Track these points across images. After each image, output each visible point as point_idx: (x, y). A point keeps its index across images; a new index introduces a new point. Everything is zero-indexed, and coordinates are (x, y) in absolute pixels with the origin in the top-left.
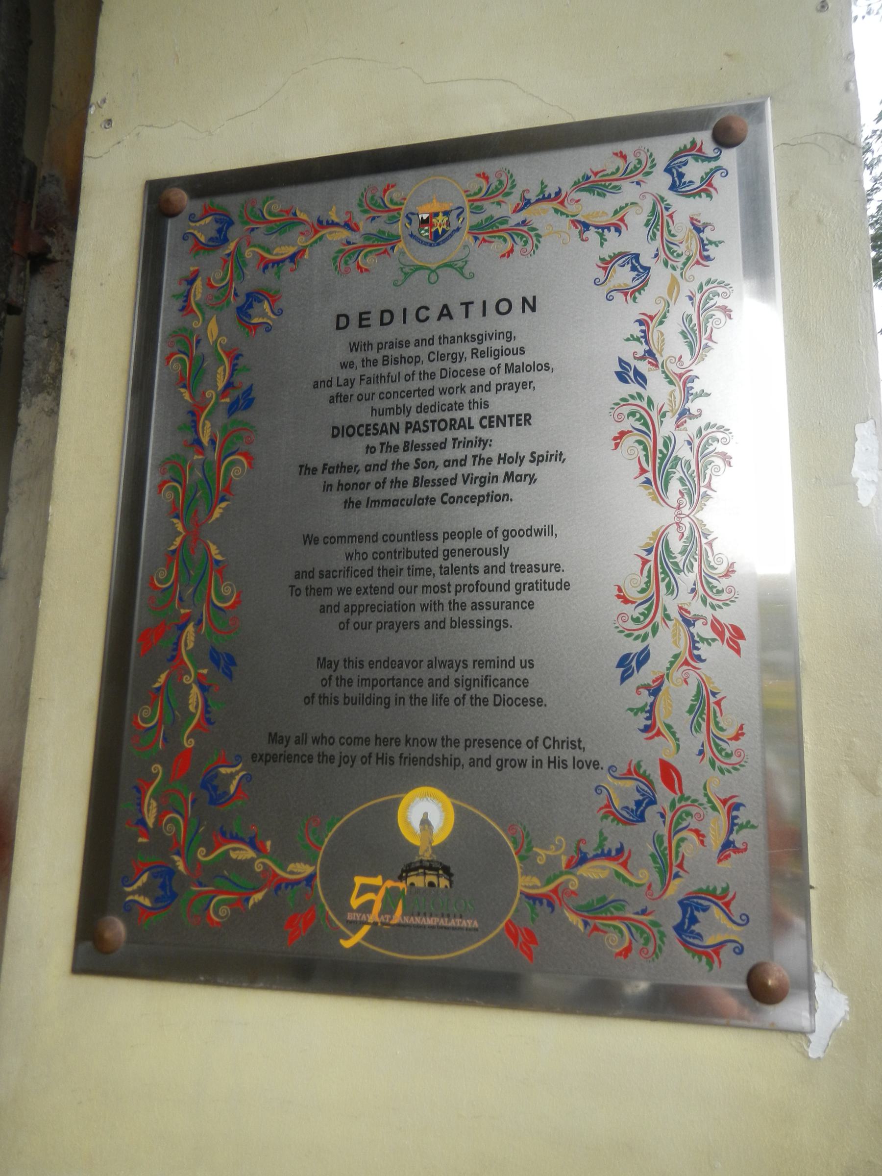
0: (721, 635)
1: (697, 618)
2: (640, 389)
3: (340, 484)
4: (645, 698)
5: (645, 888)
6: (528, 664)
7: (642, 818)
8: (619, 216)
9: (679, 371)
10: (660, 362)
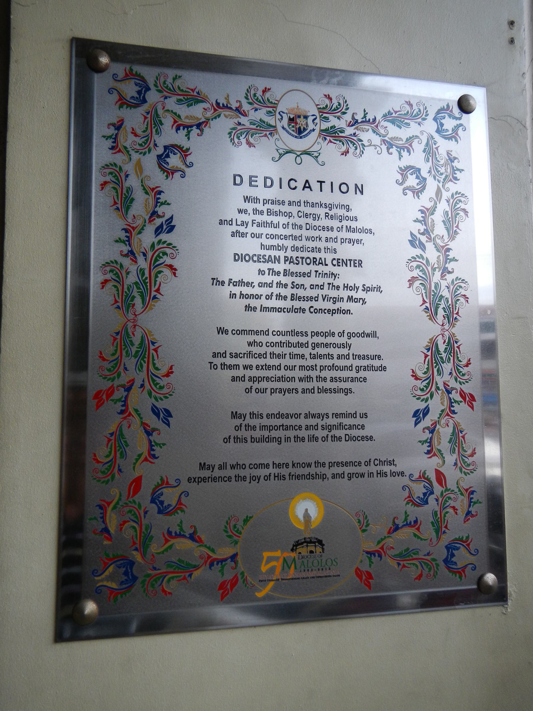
0: (464, 399)
1: (453, 389)
2: (422, 253)
3: (241, 294)
4: (427, 435)
5: (429, 541)
6: (364, 416)
7: (427, 503)
9: (442, 244)
10: (432, 237)
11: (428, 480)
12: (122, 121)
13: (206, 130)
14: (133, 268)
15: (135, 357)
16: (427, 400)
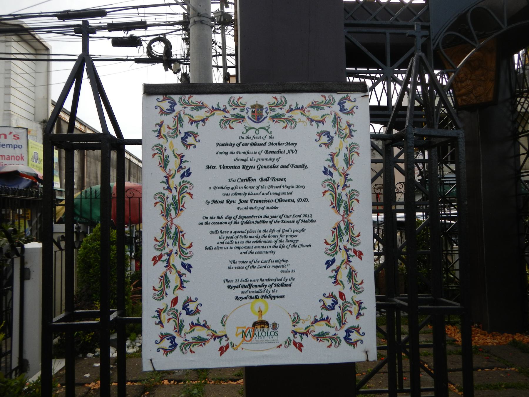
1: (349, 249)
13: (207, 122)
14: (170, 196)
15: (172, 238)
16: (333, 255)
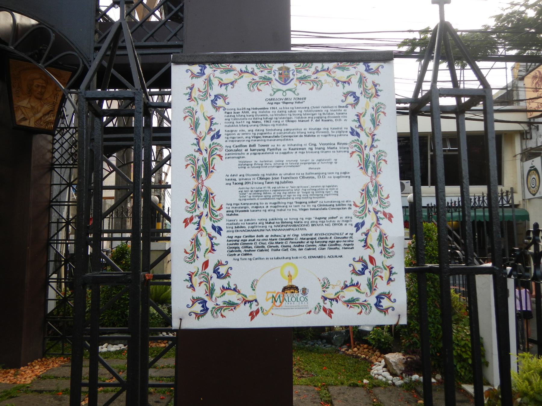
1: (379, 211)
8: (349, 78)
11: (364, 261)
12: (193, 85)
13: (235, 85)
14: (201, 157)
15: (202, 200)
16: (363, 218)
